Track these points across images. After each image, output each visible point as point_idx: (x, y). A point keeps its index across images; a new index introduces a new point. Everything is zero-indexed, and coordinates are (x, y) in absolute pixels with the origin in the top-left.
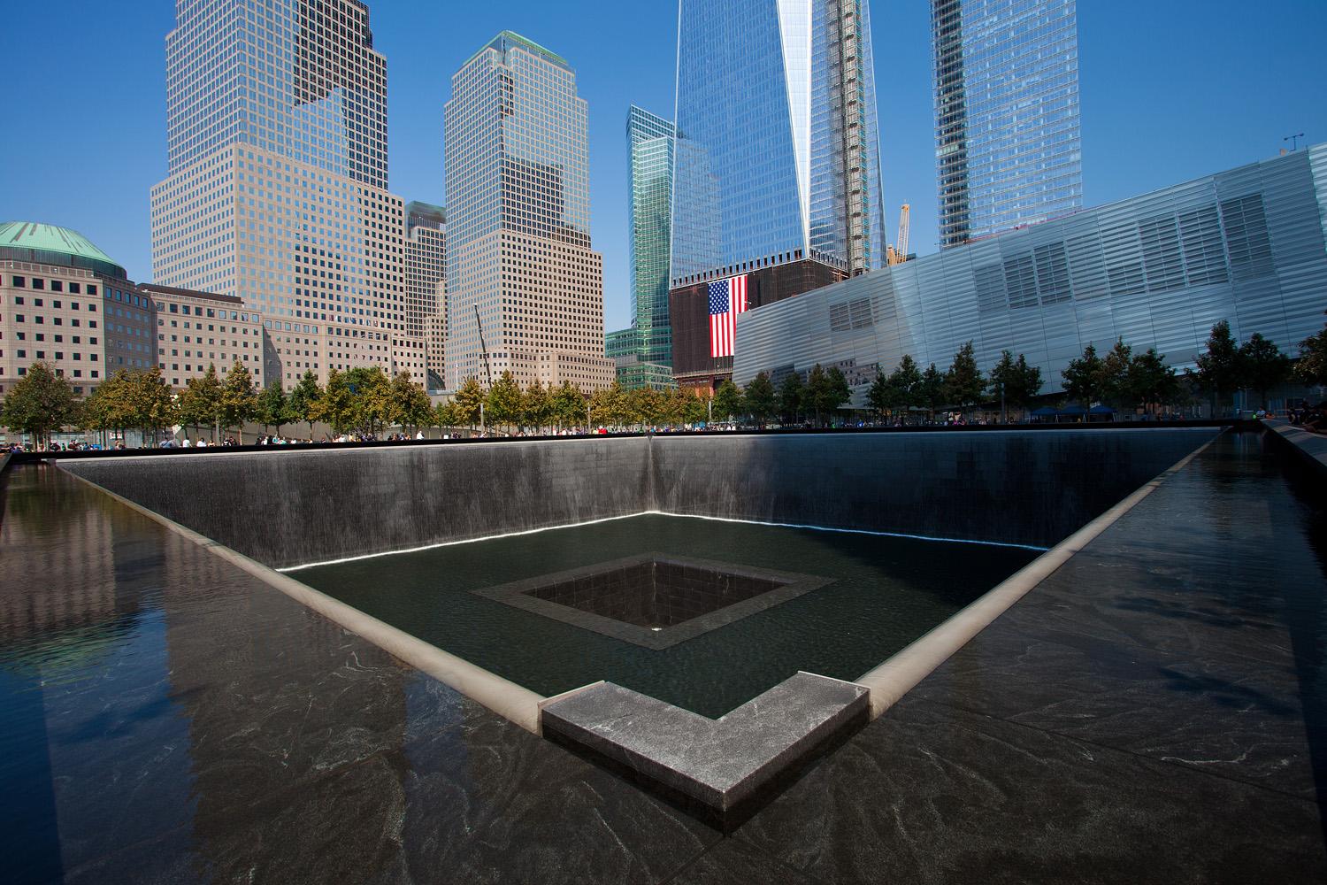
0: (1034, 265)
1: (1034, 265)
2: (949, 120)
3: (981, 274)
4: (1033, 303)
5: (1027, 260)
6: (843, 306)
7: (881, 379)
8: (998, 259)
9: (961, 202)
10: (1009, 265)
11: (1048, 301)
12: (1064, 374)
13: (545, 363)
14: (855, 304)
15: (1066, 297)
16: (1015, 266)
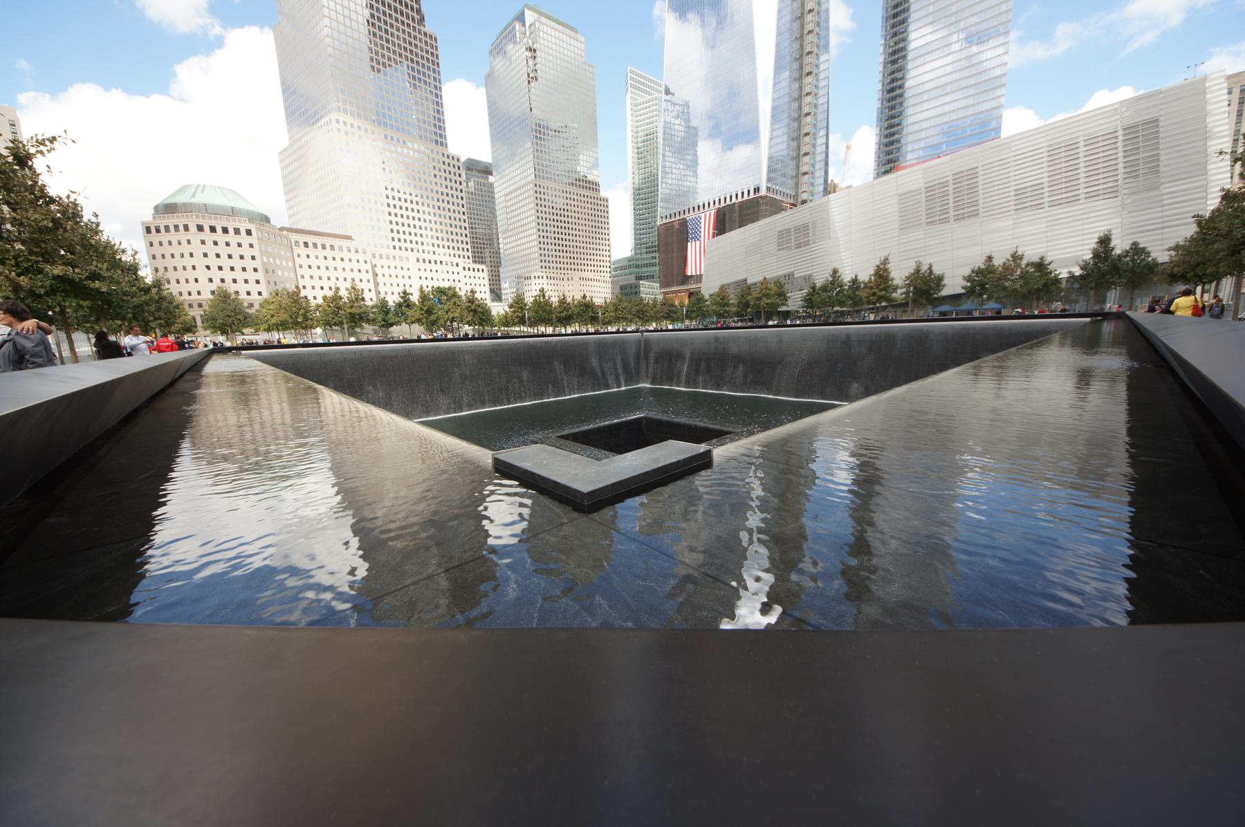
0: (951, 187)
1: (951, 187)
2: (895, 16)
3: (904, 199)
4: (945, 221)
5: (945, 184)
6: (788, 231)
7: (813, 288)
8: (920, 184)
9: (901, 46)
10: (929, 189)
11: (958, 219)
12: (965, 278)
13: (570, 282)
14: (797, 229)
15: (975, 214)
16: (934, 192)
